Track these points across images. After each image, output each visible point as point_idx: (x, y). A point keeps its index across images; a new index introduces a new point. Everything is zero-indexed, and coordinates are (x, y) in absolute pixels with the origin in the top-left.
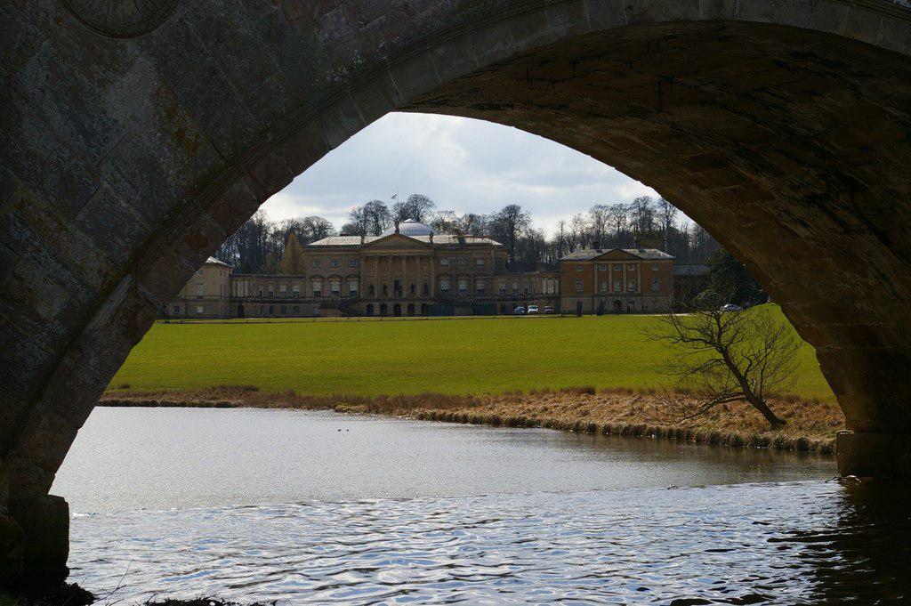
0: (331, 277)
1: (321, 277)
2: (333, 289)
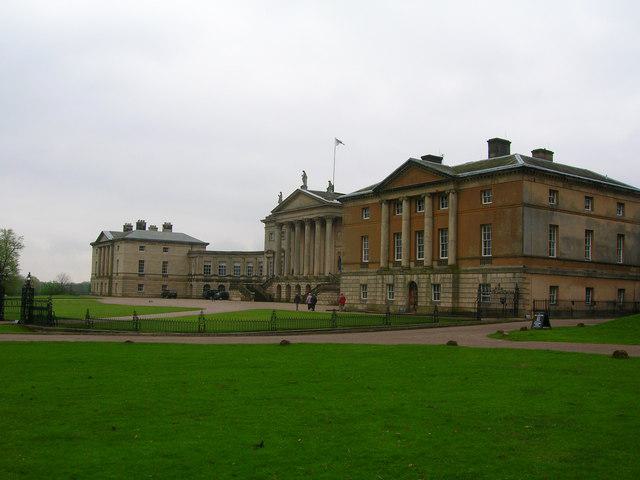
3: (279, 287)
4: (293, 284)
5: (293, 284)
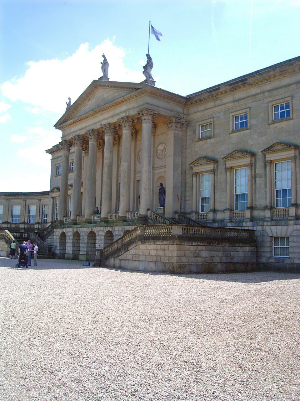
3: (63, 235)
4: (84, 231)
5: (84, 231)
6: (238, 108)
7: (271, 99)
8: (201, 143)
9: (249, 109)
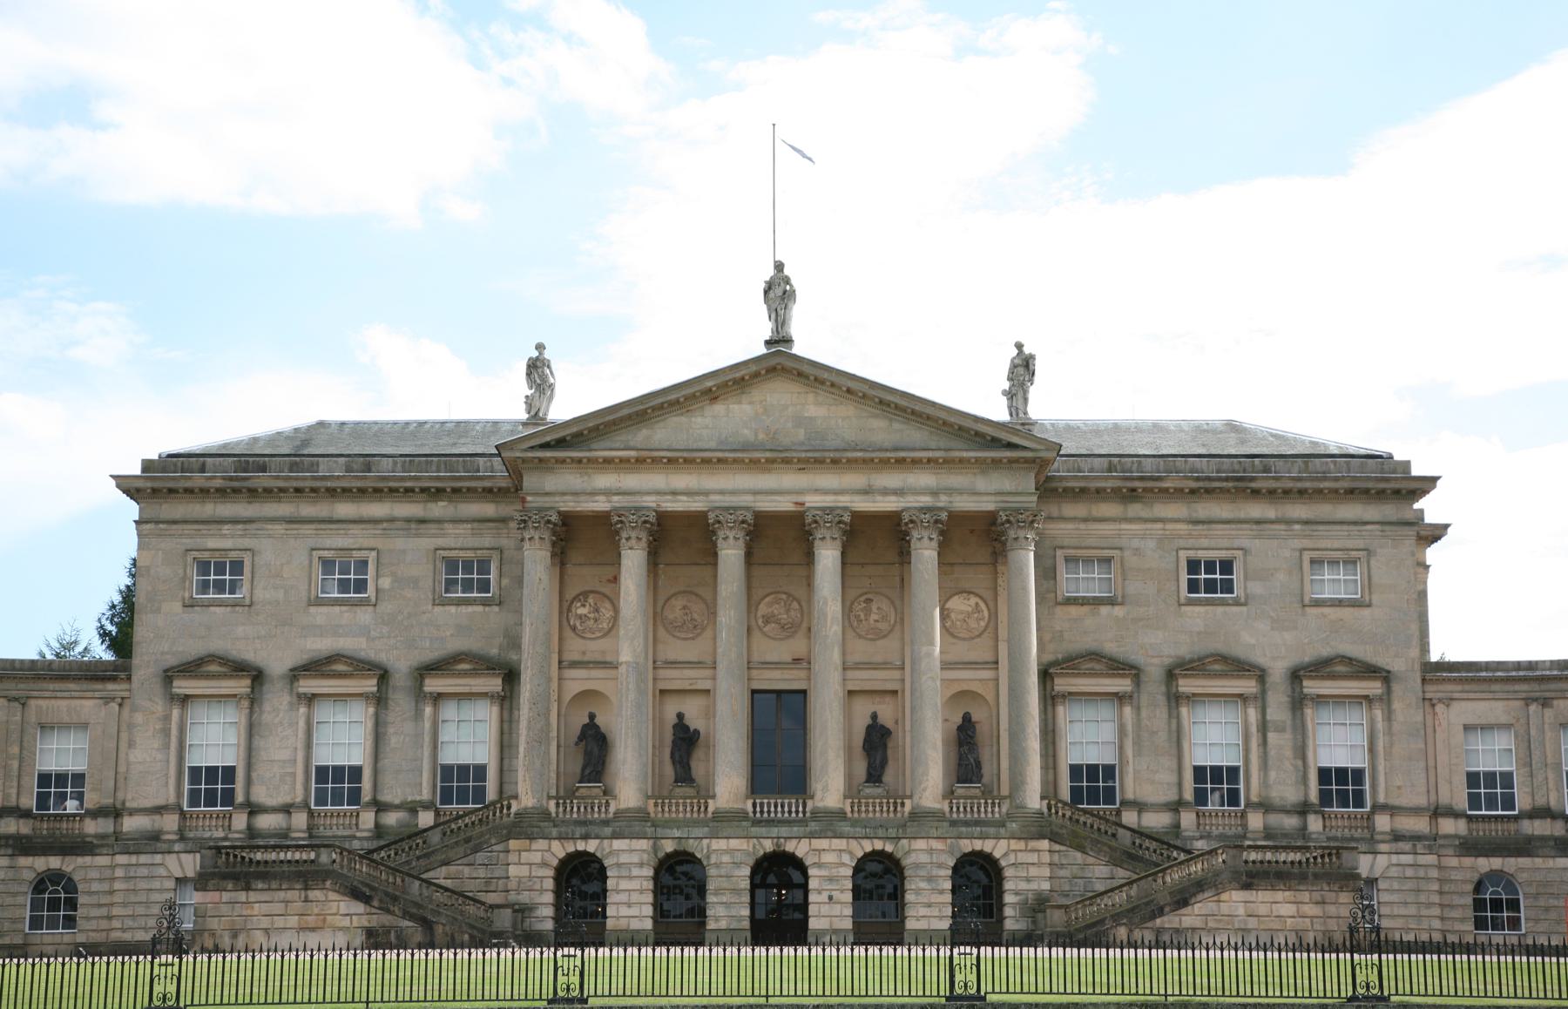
0: (317, 666)
1: (239, 668)
2: (327, 756)
6: (1205, 542)
7: (1307, 543)
8: (1074, 611)
9: (1240, 552)
